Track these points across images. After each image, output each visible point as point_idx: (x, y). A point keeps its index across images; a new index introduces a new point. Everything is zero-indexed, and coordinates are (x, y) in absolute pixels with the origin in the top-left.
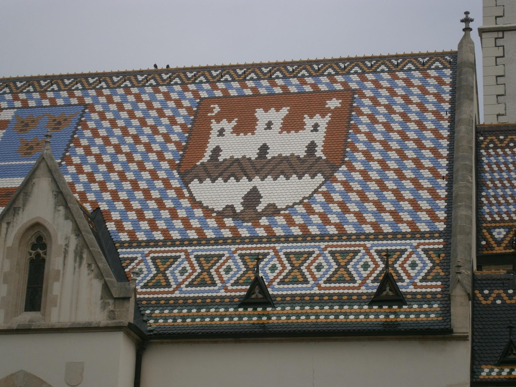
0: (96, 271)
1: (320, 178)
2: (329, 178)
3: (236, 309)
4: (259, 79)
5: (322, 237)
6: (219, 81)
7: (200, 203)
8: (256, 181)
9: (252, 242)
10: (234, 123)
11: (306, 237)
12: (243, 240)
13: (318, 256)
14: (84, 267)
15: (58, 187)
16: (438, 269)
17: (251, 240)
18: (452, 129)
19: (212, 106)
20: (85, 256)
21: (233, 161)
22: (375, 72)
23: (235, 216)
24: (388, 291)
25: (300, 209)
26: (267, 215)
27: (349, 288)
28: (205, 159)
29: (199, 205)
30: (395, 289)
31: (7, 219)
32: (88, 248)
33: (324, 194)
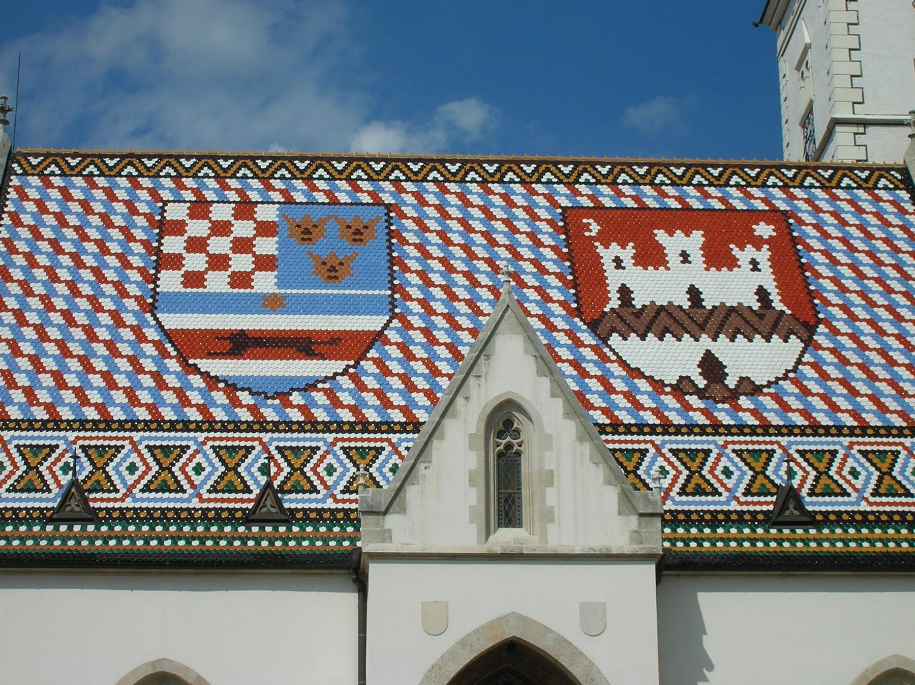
1: (795, 344)
4: (636, 183)
5: (840, 430)
7: (638, 369)
8: (705, 341)
11: (815, 429)
13: (846, 456)
17: (741, 429)
19: (585, 221)
22: (801, 186)
23: (701, 394)
25: (787, 385)
26: (746, 394)
28: (614, 303)
29: (636, 373)
33: (815, 366)
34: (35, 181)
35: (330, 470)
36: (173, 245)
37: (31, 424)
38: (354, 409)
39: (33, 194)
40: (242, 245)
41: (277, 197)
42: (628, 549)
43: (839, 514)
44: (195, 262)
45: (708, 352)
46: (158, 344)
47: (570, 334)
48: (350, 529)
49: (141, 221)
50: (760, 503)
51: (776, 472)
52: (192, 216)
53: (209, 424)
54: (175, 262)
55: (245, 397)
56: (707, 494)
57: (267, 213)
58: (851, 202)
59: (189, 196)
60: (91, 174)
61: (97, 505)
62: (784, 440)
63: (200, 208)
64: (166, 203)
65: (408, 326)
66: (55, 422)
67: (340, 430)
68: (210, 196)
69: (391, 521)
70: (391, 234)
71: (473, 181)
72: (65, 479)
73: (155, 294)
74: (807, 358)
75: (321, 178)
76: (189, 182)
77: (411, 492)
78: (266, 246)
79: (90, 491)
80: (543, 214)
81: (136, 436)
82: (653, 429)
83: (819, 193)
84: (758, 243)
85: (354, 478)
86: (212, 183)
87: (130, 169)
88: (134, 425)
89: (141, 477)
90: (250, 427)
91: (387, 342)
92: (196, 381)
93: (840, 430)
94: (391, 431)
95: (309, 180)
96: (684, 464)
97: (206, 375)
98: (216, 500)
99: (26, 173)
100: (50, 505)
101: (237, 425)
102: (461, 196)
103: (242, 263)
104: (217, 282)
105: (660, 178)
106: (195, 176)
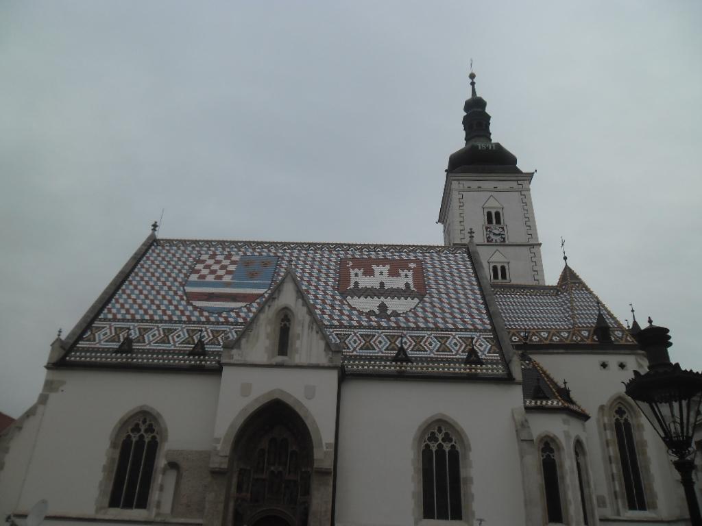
2: (422, 300)
3: (391, 363)
5: (428, 329)
6: (348, 250)
8: (382, 299)
10: (362, 270)
11: (418, 328)
12: (384, 328)
14: (314, 332)
17: (389, 328)
20: (314, 327)
21: (367, 289)
24: (473, 357)
25: (410, 314)
27: (450, 355)
28: (352, 286)
29: (354, 309)
30: (478, 357)
31: (268, 304)
32: (316, 323)
36: (199, 266)
37: (124, 320)
40: (223, 267)
41: (241, 253)
45: (383, 303)
50: (391, 353)
53: (189, 321)
55: (206, 314)
56: (370, 349)
57: (235, 258)
59: (211, 253)
62: (405, 332)
63: (213, 256)
64: (201, 254)
66: (133, 320)
68: (218, 253)
69: (234, 352)
71: (312, 250)
73: (186, 281)
74: (420, 305)
76: (212, 249)
77: (243, 341)
81: (160, 325)
82: (355, 327)
84: (409, 269)
86: (220, 249)
88: (161, 321)
90: (203, 323)
92: (190, 308)
95: (254, 249)
99: (158, 245)
101: (199, 322)
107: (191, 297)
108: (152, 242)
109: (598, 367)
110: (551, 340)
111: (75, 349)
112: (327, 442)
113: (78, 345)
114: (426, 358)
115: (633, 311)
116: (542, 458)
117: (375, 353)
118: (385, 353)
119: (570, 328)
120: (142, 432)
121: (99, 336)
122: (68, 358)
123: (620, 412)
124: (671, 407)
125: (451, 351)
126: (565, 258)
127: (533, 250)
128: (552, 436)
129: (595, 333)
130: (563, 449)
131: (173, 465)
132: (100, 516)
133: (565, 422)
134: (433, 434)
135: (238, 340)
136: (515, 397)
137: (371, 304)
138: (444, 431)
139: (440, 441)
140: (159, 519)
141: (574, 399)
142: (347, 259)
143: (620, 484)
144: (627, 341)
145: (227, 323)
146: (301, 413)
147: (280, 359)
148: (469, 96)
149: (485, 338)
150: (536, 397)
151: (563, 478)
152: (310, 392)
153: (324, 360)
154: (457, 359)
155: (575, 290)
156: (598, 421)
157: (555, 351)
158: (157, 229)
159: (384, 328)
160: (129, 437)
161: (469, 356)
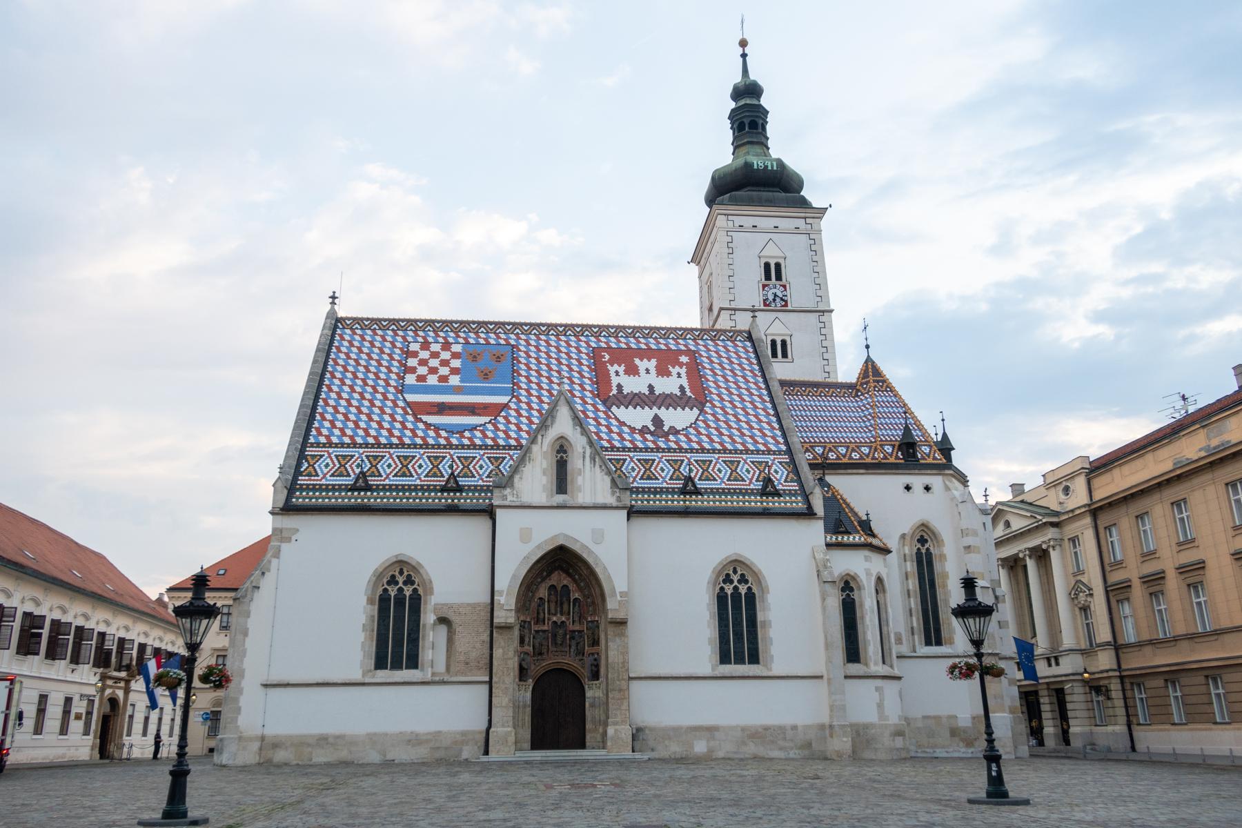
0: (605, 470)
2: (702, 411)
3: (679, 496)
4: (627, 337)
5: (714, 451)
7: (624, 422)
8: (655, 410)
9: (669, 452)
10: (623, 367)
11: (703, 450)
12: (663, 450)
15: (574, 413)
16: (791, 475)
17: (669, 450)
18: (766, 382)
20: (597, 460)
22: (702, 339)
23: (651, 433)
24: (769, 488)
25: (691, 430)
26: (672, 434)
28: (614, 391)
29: (622, 424)
30: (774, 486)
31: (541, 433)
32: (599, 455)
33: (704, 422)
34: (348, 331)
35: (481, 467)
36: (412, 362)
37: (342, 445)
38: (493, 439)
39: (347, 337)
40: (445, 363)
41: (461, 340)
42: (615, 504)
43: (712, 489)
44: (422, 370)
45: (656, 414)
46: (403, 409)
47: (594, 405)
48: (489, 494)
49: (397, 351)
50: (677, 484)
51: (684, 470)
52: (421, 349)
53: (426, 445)
54: (413, 370)
55: (443, 433)
57: (457, 348)
58: (724, 347)
59: (420, 339)
60: (375, 329)
61: (372, 483)
62: (689, 455)
63: (425, 345)
64: (409, 343)
65: (520, 401)
66: (354, 444)
67: (486, 449)
68: (430, 340)
69: (508, 490)
70: (514, 359)
71: (552, 334)
72: (357, 471)
73: (403, 385)
74: (701, 418)
75: (482, 332)
76: (421, 333)
78: (456, 363)
79: (369, 476)
80: (584, 350)
82: (629, 450)
83: (710, 342)
84: (681, 365)
85: (491, 471)
86: (431, 334)
87: (393, 327)
88: (391, 445)
89: (393, 470)
90: (445, 447)
91: (511, 409)
93: (714, 451)
94: (510, 449)
95: (476, 333)
96: (643, 465)
97: (425, 423)
98: (428, 481)
99: (344, 328)
100: (350, 483)
101: (439, 446)
102: (546, 342)
103: (444, 371)
104: (432, 380)
105: (638, 334)
106: (424, 330)
107: (418, 409)
108: (335, 324)
109: (902, 488)
110: (851, 458)
111: (298, 487)
112: (622, 590)
113: (299, 482)
114: (718, 489)
115: (943, 420)
116: (841, 598)
117: (659, 484)
118: (671, 484)
119: (871, 442)
120: (401, 585)
121: (320, 467)
122: (294, 500)
123: (922, 541)
124: (975, 620)
125: (743, 480)
126: (867, 347)
127: (822, 318)
128: (852, 574)
129: (900, 448)
130: (864, 589)
131: (443, 620)
132: (367, 680)
133: (867, 559)
134: (728, 575)
135: (511, 477)
136: (814, 533)
137: (640, 417)
138: (739, 573)
139: (736, 583)
140: (437, 679)
141: (876, 532)
142: (600, 348)
143: (918, 619)
144: (935, 458)
145: (473, 446)
146: (590, 560)
147: (560, 499)
148: (737, 78)
149: (780, 463)
150: (837, 532)
151: (863, 618)
152: (598, 536)
153: (611, 500)
154: (752, 490)
155: (878, 391)
156: (899, 552)
157: (855, 471)
158: (336, 301)
159: (663, 450)
160: (385, 590)
161: (765, 487)
